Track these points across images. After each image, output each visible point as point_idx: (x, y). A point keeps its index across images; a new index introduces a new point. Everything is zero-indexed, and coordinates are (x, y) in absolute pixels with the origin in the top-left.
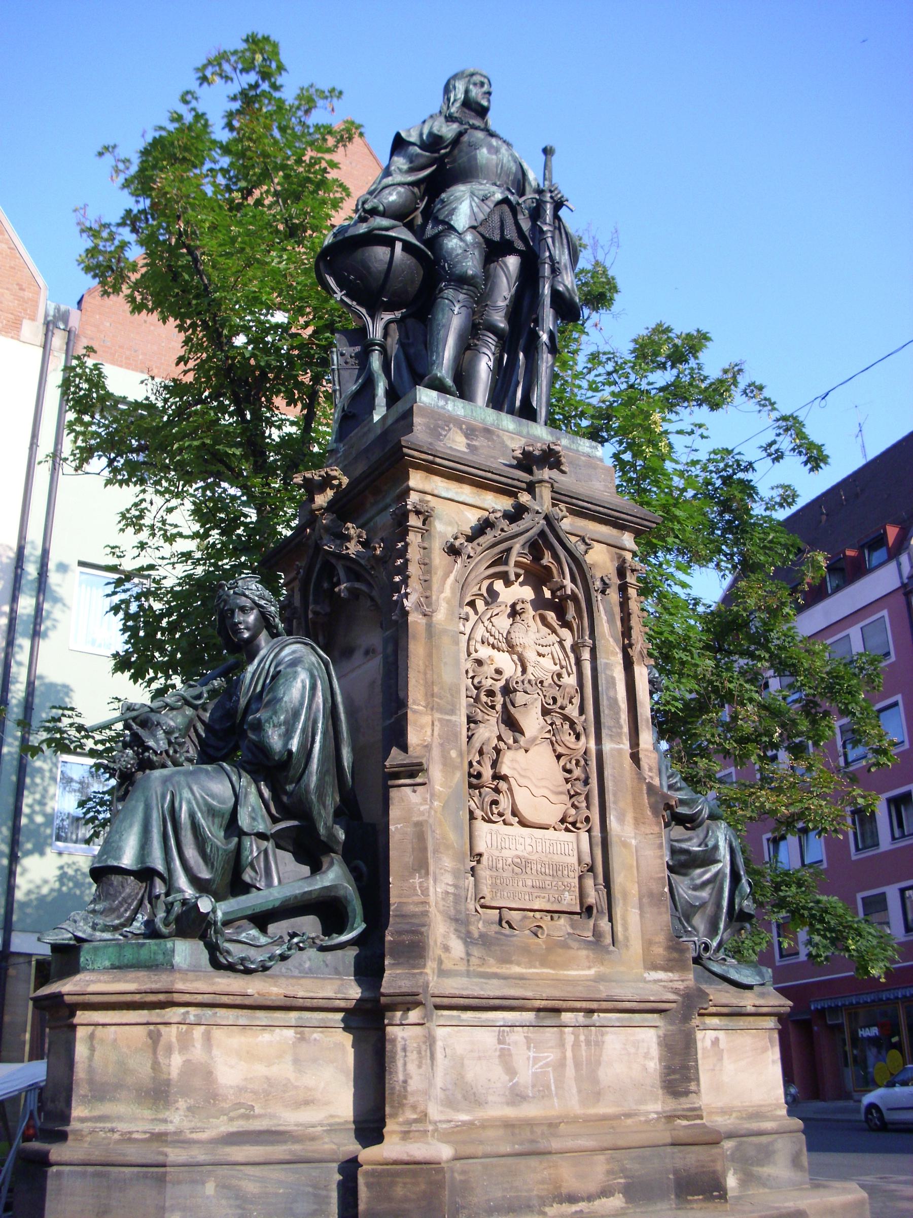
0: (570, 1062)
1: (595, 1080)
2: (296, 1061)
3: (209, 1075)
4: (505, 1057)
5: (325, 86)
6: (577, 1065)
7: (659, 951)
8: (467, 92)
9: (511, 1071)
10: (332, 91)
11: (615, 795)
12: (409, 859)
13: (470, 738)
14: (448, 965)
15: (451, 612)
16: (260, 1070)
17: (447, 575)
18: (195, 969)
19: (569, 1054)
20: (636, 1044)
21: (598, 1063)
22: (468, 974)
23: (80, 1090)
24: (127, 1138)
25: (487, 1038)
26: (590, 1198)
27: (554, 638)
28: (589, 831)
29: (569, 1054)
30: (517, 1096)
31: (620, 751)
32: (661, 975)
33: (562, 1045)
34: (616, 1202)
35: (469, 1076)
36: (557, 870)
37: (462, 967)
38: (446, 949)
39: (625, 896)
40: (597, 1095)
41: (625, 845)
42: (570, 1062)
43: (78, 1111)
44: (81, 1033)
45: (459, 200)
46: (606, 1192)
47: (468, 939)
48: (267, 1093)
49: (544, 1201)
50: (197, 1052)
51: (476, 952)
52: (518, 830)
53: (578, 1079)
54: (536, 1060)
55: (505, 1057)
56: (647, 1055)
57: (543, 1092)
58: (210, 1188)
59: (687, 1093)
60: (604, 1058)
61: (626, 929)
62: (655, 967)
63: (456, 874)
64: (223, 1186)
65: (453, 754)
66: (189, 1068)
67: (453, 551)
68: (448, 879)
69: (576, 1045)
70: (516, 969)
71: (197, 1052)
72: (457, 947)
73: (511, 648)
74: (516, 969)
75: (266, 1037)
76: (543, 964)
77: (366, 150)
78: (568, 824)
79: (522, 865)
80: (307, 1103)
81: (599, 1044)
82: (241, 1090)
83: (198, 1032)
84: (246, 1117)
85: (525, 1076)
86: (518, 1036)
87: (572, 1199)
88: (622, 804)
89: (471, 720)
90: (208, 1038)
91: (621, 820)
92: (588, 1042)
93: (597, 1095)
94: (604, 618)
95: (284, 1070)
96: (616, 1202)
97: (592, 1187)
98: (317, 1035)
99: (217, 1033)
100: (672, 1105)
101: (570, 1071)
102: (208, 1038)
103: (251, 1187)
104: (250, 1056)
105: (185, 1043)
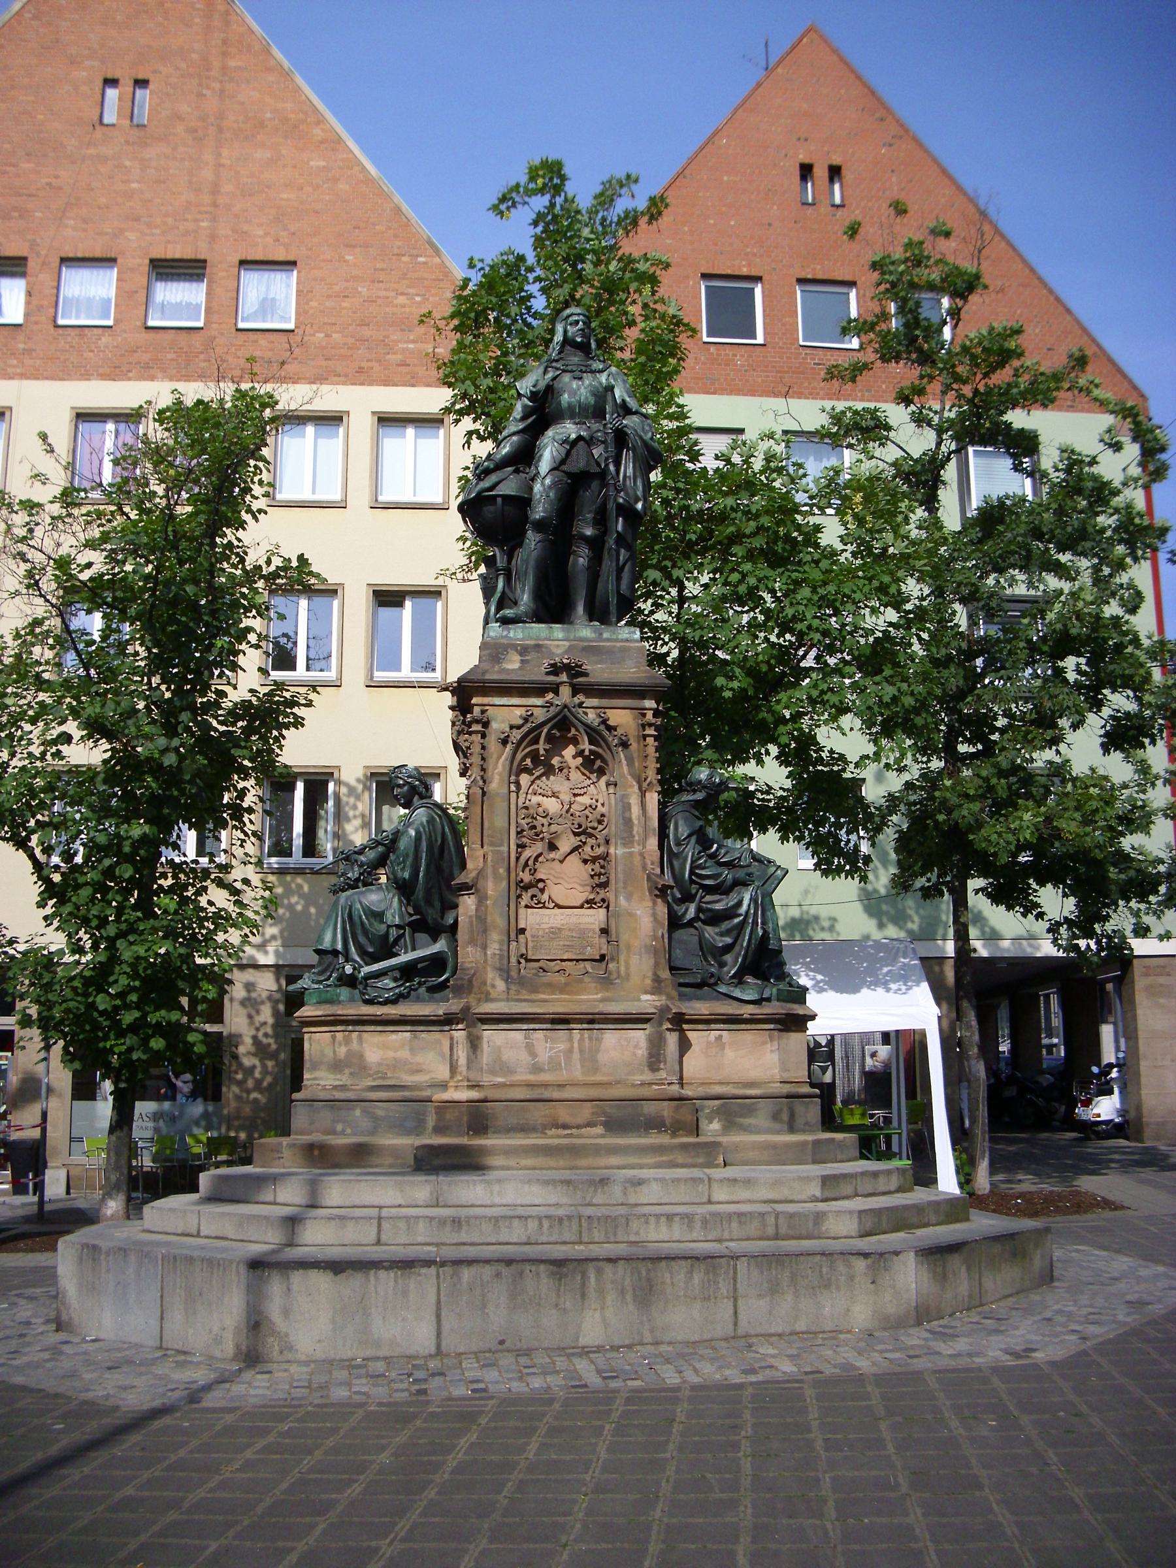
0: (576, 1049)
1: (594, 1060)
2: (411, 1049)
3: (361, 1056)
4: (531, 1049)
5: (622, 175)
6: (581, 1051)
7: (648, 982)
8: (565, 332)
9: (533, 1055)
10: (628, 177)
11: (625, 882)
12: (466, 937)
13: (518, 859)
14: (494, 995)
15: (501, 780)
16: (391, 1054)
17: (499, 757)
18: (352, 1000)
19: (576, 1045)
20: (628, 1040)
21: (598, 1051)
22: (508, 1000)
23: (307, 1065)
24: (324, 1088)
25: (518, 1036)
26: (578, 1127)
27: (588, 782)
28: (607, 908)
29: (576, 1045)
30: (536, 1069)
31: (631, 854)
32: (648, 997)
33: (571, 1039)
34: (599, 1130)
35: (504, 1058)
36: (582, 933)
37: (504, 996)
38: (493, 986)
39: (628, 947)
40: (596, 1070)
41: (632, 915)
42: (576, 1049)
43: (306, 1076)
44: (306, 1036)
45: (545, 446)
46: (590, 1124)
47: (507, 979)
48: (395, 1067)
49: (545, 1127)
50: (355, 1045)
51: (513, 987)
52: (557, 911)
53: (582, 1060)
54: (551, 1049)
55: (531, 1049)
56: (636, 1047)
57: (555, 1065)
58: (358, 1112)
59: (658, 1070)
60: (603, 1046)
61: (627, 967)
62: (646, 993)
63: (501, 942)
64: (364, 1111)
65: (501, 871)
66: (350, 1054)
67: (505, 742)
68: (496, 946)
69: (581, 1040)
70: (542, 996)
71: (355, 1045)
72: (501, 985)
73: (554, 795)
74: (542, 996)
75: (394, 1037)
76: (562, 992)
77: (835, 58)
78: (590, 903)
79: (555, 933)
80: (419, 1071)
81: (600, 1041)
82: (380, 1064)
83: (355, 1035)
84: (383, 1078)
85: (544, 1056)
86: (540, 1034)
87: (565, 1126)
88: (630, 888)
89: (521, 846)
90: (360, 1039)
91: (629, 898)
92: (590, 1039)
93: (596, 1070)
94: (624, 762)
95: (404, 1054)
96: (599, 1130)
97: (580, 1120)
98: (424, 1035)
99: (365, 1035)
100: (648, 1076)
101: (576, 1055)
102: (360, 1039)
103: (380, 1113)
104: (385, 1047)
105: (347, 1041)
